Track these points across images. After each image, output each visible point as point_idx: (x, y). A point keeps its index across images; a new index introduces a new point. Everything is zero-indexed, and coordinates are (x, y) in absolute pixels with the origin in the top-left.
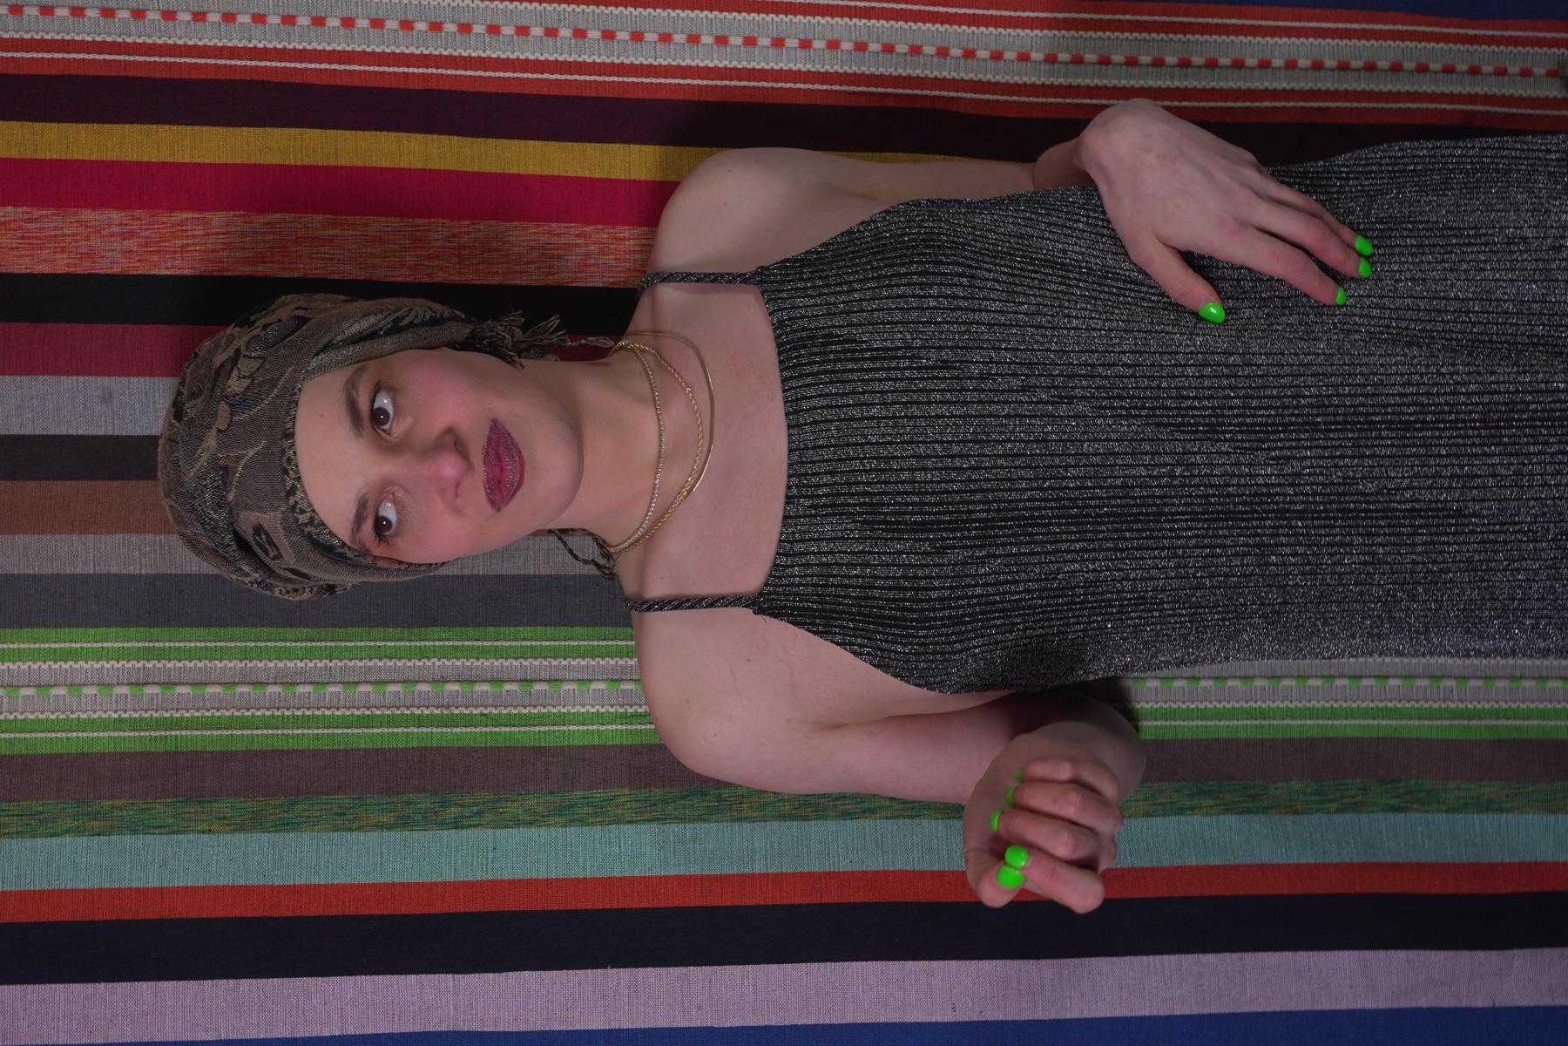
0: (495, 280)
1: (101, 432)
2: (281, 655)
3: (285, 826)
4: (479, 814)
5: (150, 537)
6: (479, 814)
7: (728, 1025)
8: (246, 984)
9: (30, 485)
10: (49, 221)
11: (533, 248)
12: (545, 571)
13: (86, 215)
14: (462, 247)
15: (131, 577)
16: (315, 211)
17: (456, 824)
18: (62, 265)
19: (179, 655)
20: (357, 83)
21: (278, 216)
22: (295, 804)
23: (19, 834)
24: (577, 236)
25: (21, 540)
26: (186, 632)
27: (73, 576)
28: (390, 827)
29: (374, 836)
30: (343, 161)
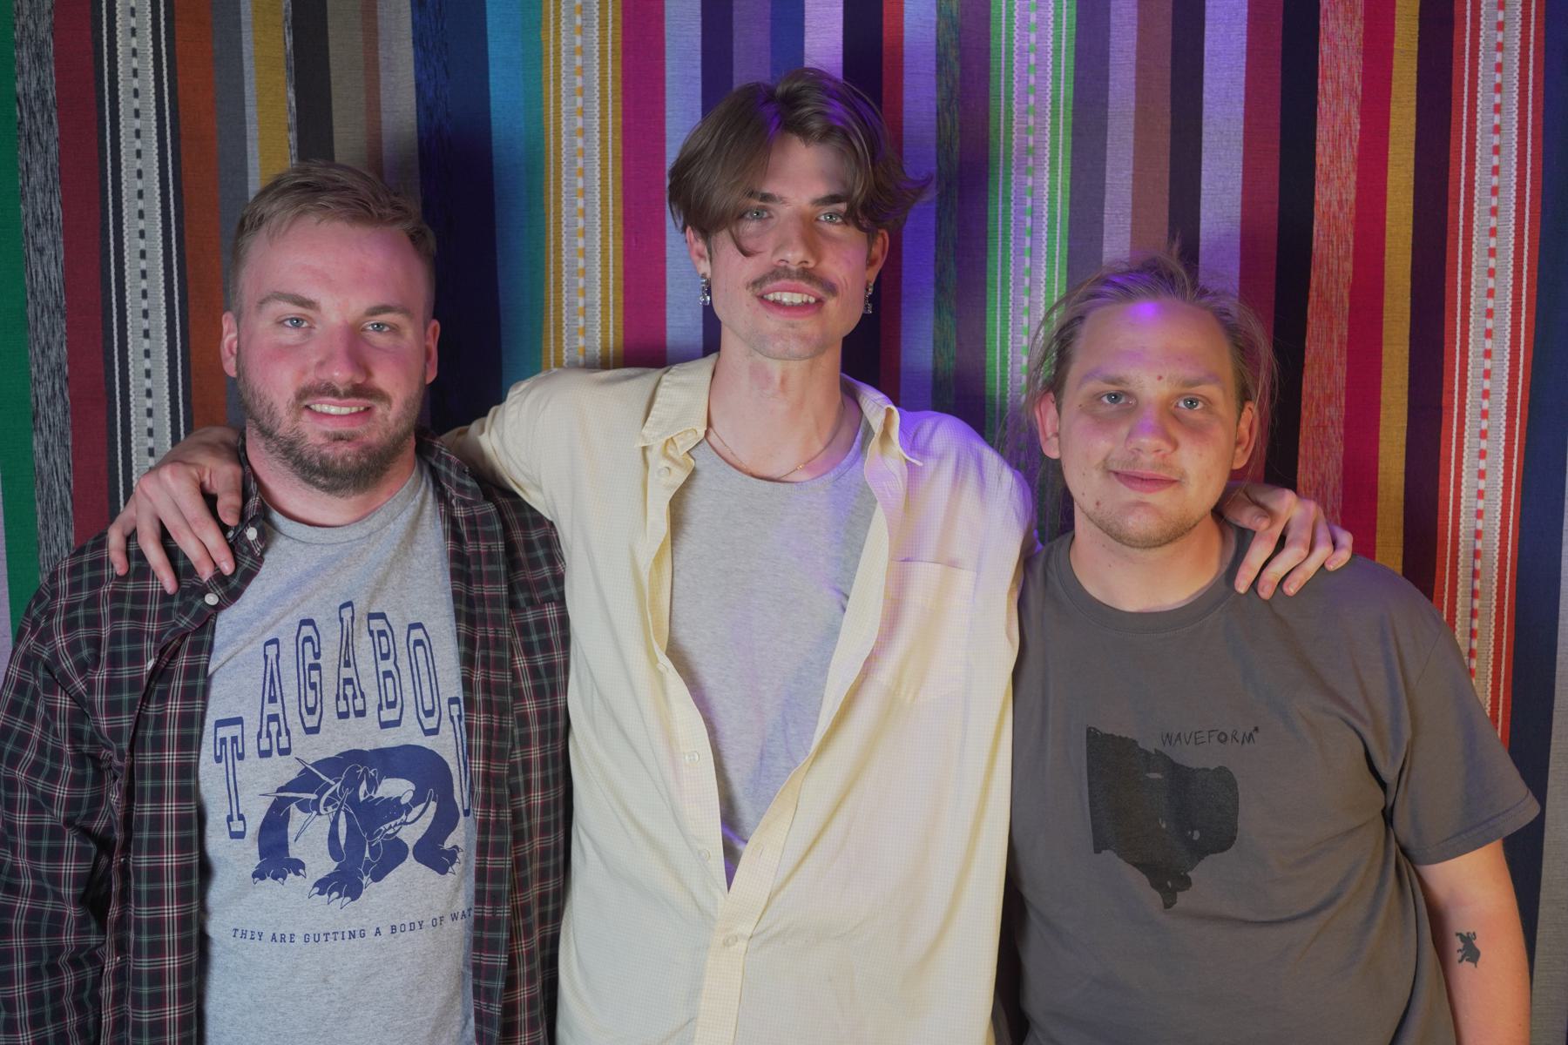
0: (1302, 450)
1: (1203, 186)
5: (1129, 221)
9: (1167, 140)
11: (1323, 476)
14: (1325, 428)
15: (1101, 208)
18: (1322, 160)
23: (939, 137)
25: (1131, 137)
26: (1065, 244)
27: (1104, 169)
30: (1386, 350)
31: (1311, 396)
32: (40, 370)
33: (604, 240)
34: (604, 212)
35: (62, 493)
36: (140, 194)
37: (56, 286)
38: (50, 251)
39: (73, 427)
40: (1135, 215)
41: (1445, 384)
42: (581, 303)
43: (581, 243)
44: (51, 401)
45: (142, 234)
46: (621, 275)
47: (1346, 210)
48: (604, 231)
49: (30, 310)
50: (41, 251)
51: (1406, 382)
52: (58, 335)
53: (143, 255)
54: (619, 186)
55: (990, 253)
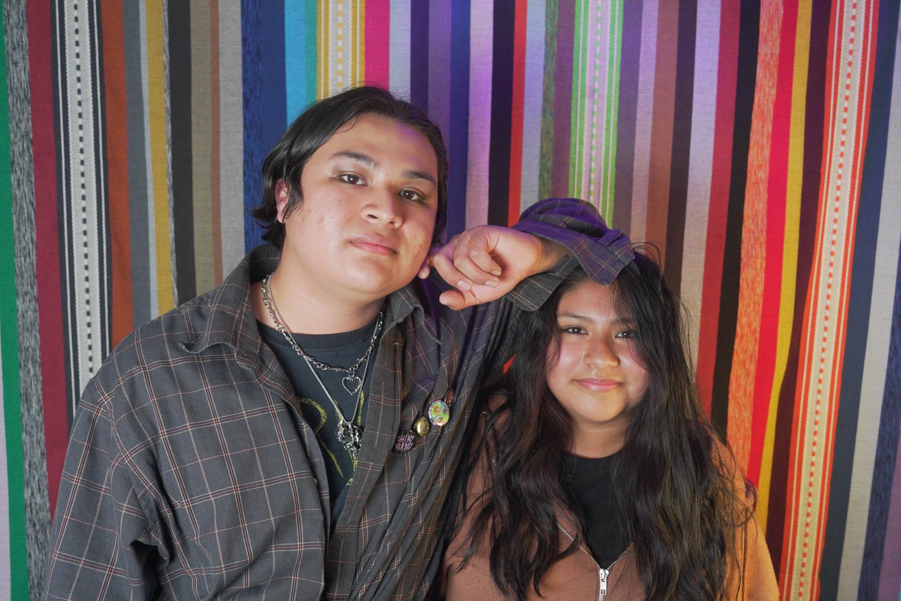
2: (609, 111)
3: (544, 110)
4: (544, 185)
5: (654, 62)
6: (544, 185)
8: (490, 96)
10: (777, 26)
12: (633, 213)
13: (779, 40)
14: (758, 184)
15: (638, 54)
16: (774, 128)
17: (541, 176)
19: (611, 72)
23: (547, 11)
25: (656, 14)
26: (619, 74)
28: (541, 151)
29: (538, 144)
31: (752, 166)
32: (15, 136)
33: (354, 66)
34: (354, 49)
35: (28, 210)
36: (77, 31)
37: (25, 85)
38: (21, 64)
39: (35, 170)
40: (658, 58)
43: (340, 67)
44: (22, 154)
45: (78, 55)
47: (774, 59)
48: (354, 60)
49: (10, 99)
50: (16, 64)
52: (26, 115)
53: (78, 68)
54: (363, 34)
55: (574, 79)
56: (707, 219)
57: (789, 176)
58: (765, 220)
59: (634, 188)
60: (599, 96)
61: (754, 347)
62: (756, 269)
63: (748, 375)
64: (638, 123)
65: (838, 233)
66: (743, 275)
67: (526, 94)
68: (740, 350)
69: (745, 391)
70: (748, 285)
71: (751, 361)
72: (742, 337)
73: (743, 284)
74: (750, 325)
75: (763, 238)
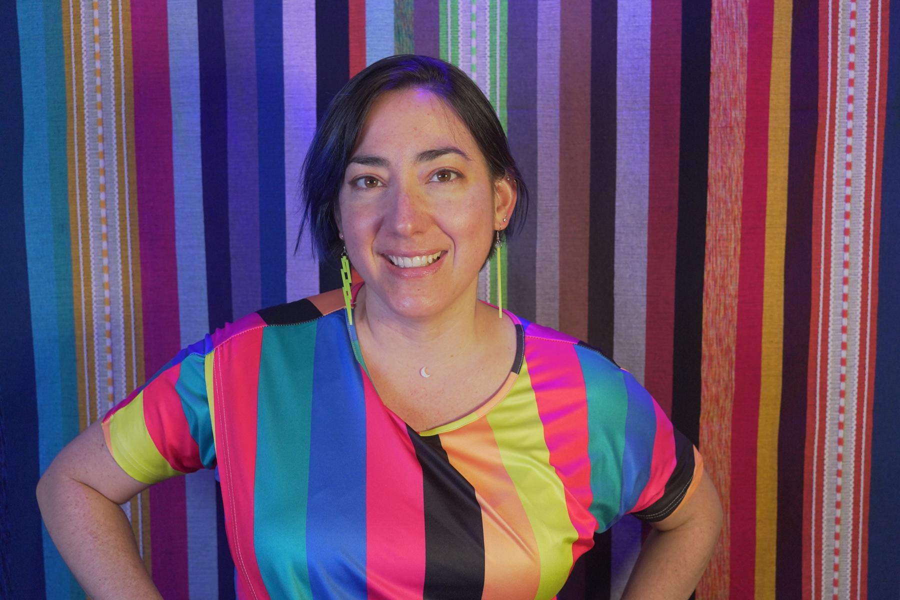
2: (493, 29)
3: (398, 32)
7: (288, 281)
8: (312, 14)
20: (820, 70)
21: (746, 22)
22: (410, 37)
24: (736, 196)
30: (774, 61)
41: (820, 91)
42: (97, 31)
46: (129, 8)
51: (788, 91)
56: (647, 184)
57: (772, 115)
58: (742, 182)
59: (540, 141)
60: (478, 8)
61: (729, 373)
62: (727, 257)
63: (722, 416)
64: (539, 44)
65: (852, 200)
66: (708, 267)
67: (367, 9)
68: (710, 381)
69: (720, 440)
70: (716, 282)
71: (726, 395)
72: (711, 358)
73: (708, 280)
74: (720, 341)
75: (737, 210)
